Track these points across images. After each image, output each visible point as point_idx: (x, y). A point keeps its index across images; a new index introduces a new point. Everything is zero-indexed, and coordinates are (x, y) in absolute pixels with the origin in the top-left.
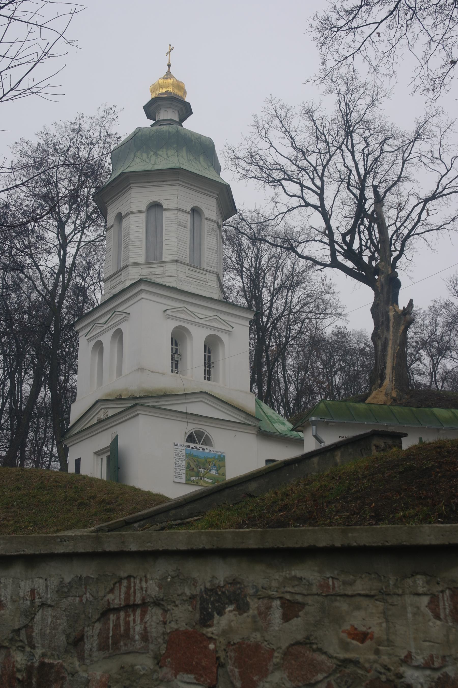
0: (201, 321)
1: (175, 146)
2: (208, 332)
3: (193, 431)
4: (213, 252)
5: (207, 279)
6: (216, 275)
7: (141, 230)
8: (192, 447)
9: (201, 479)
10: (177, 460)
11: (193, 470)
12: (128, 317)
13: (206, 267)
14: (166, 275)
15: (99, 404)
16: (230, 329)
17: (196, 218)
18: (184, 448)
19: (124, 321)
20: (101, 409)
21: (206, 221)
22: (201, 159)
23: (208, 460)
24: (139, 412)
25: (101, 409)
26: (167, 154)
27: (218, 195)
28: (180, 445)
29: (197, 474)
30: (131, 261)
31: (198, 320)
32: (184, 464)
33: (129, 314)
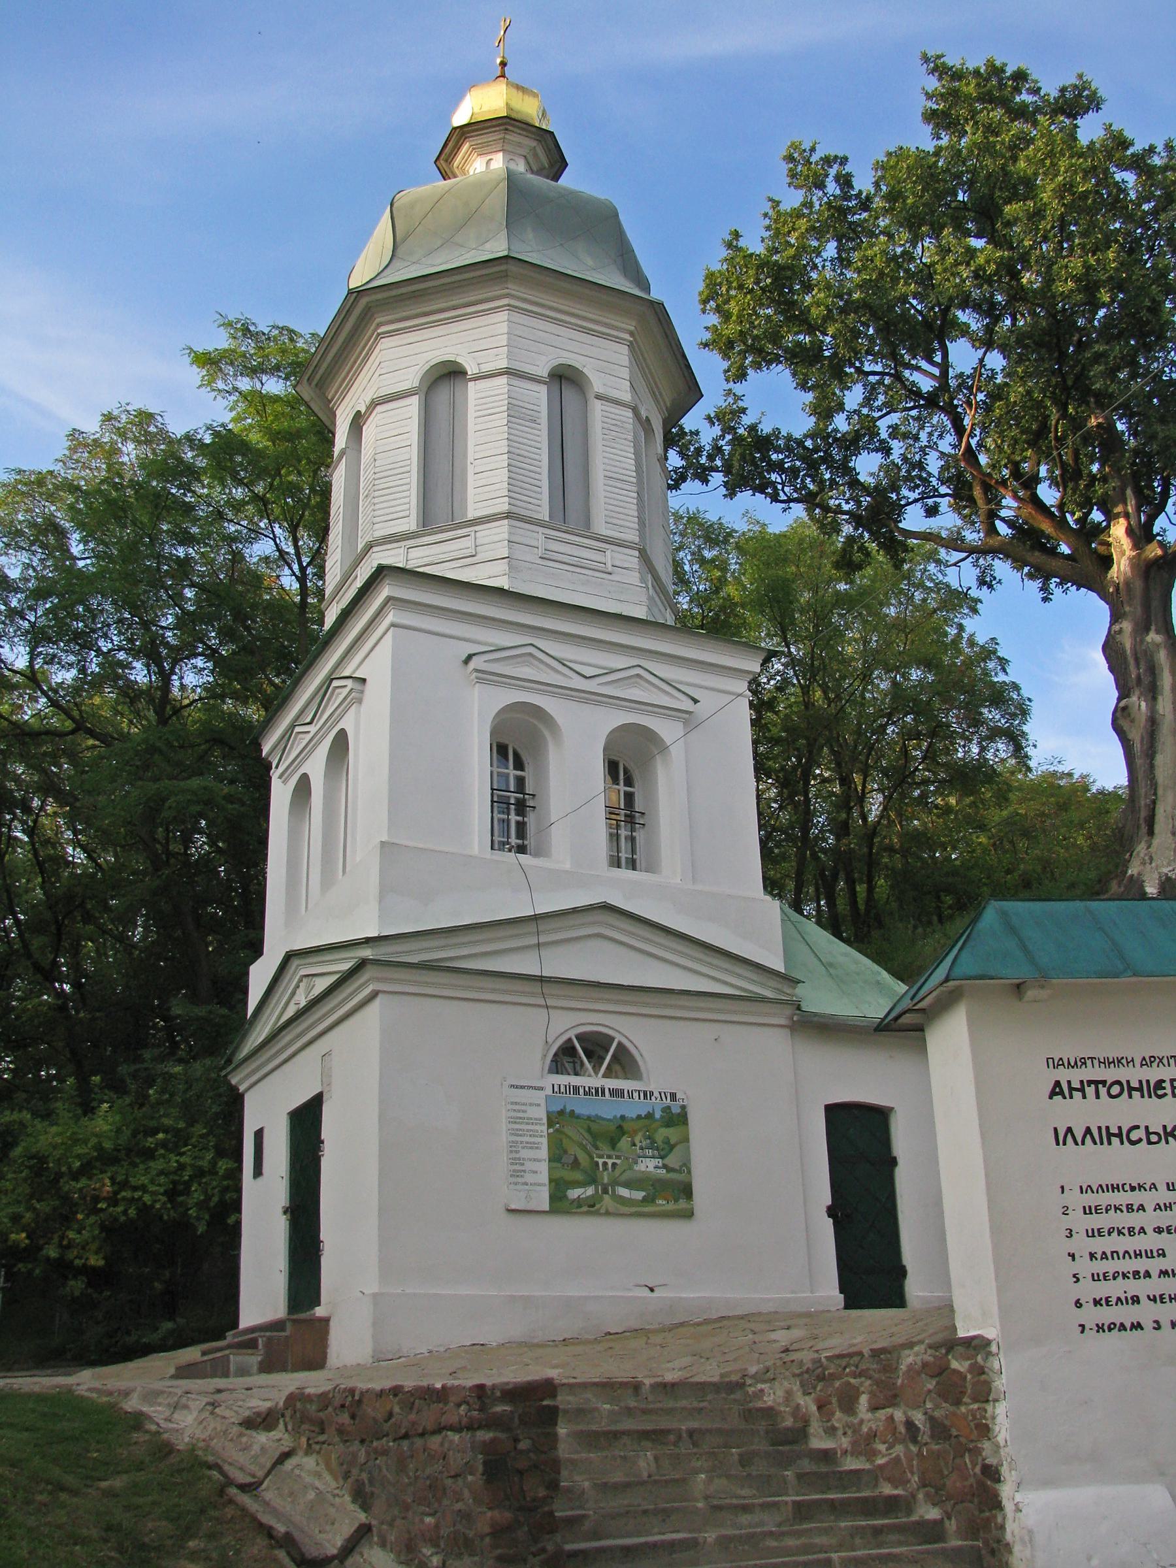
3: (572, 1034)
5: (609, 565)
6: (636, 553)
11: (576, 1164)
12: (362, 692)
15: (295, 962)
16: (687, 705)
17: (569, 393)
20: (300, 981)
21: (598, 403)
25: (300, 981)
27: (631, 334)
30: (381, 531)
33: (364, 681)
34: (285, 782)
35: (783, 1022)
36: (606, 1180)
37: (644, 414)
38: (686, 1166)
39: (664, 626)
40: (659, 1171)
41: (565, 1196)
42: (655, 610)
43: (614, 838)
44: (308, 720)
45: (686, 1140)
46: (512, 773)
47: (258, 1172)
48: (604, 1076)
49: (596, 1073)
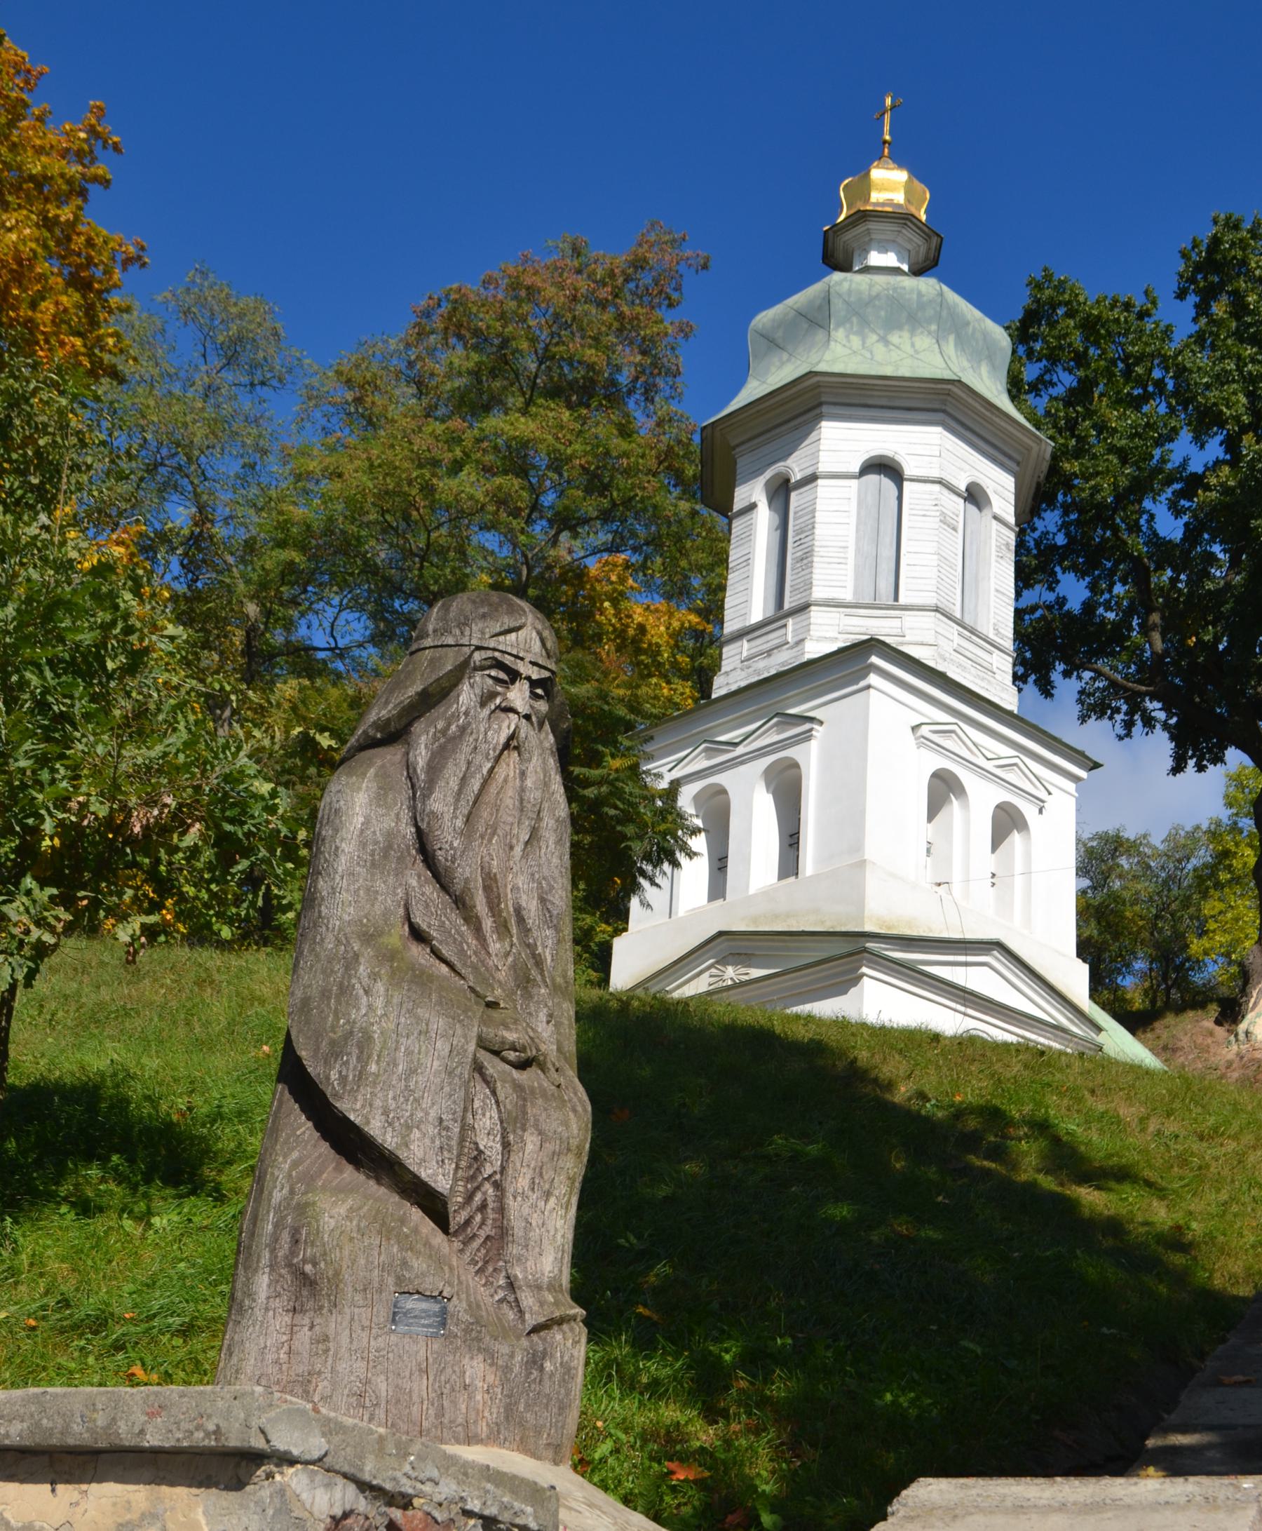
0: (989, 766)
1: (934, 327)
2: (1003, 796)
7: (847, 521)
19: (809, 739)
26: (913, 345)
30: (818, 593)
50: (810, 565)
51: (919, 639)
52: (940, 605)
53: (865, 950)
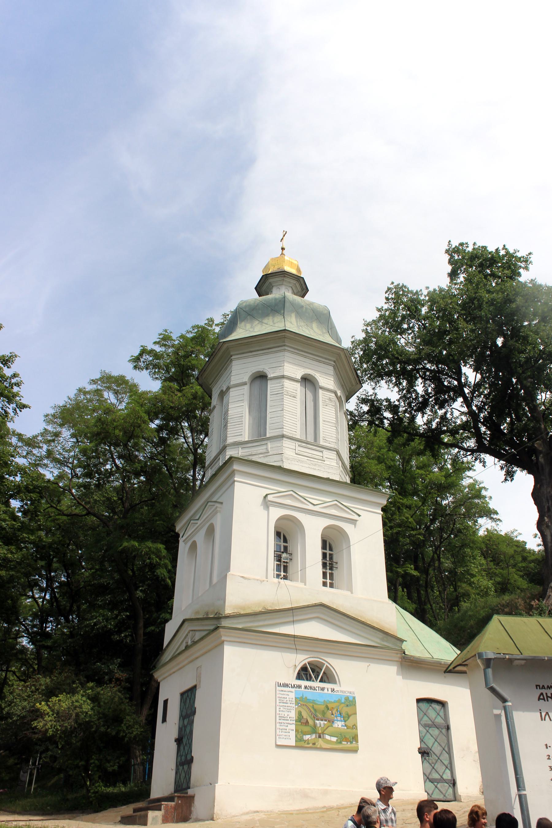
3: (306, 662)
4: (332, 425)
8: (306, 687)
9: (320, 737)
10: (282, 709)
11: (307, 723)
13: (322, 443)
14: (271, 453)
15: (186, 624)
16: (355, 517)
18: (293, 690)
19: (216, 513)
20: (189, 632)
22: (314, 325)
23: (330, 706)
24: (223, 638)
26: (273, 321)
27: (334, 362)
28: (286, 685)
29: (314, 730)
31: (311, 507)
32: (293, 714)
33: (222, 503)
34: (186, 544)
35: (397, 659)
36: (320, 732)
37: (339, 394)
38: (355, 727)
39: (346, 483)
40: (343, 728)
41: (303, 738)
42: (343, 476)
43: (324, 575)
44: (197, 518)
45: (355, 714)
46: (282, 544)
47: (164, 720)
48: (320, 681)
49: (317, 679)
50: (227, 429)
51: (275, 452)
52: (285, 433)
53: (218, 627)
